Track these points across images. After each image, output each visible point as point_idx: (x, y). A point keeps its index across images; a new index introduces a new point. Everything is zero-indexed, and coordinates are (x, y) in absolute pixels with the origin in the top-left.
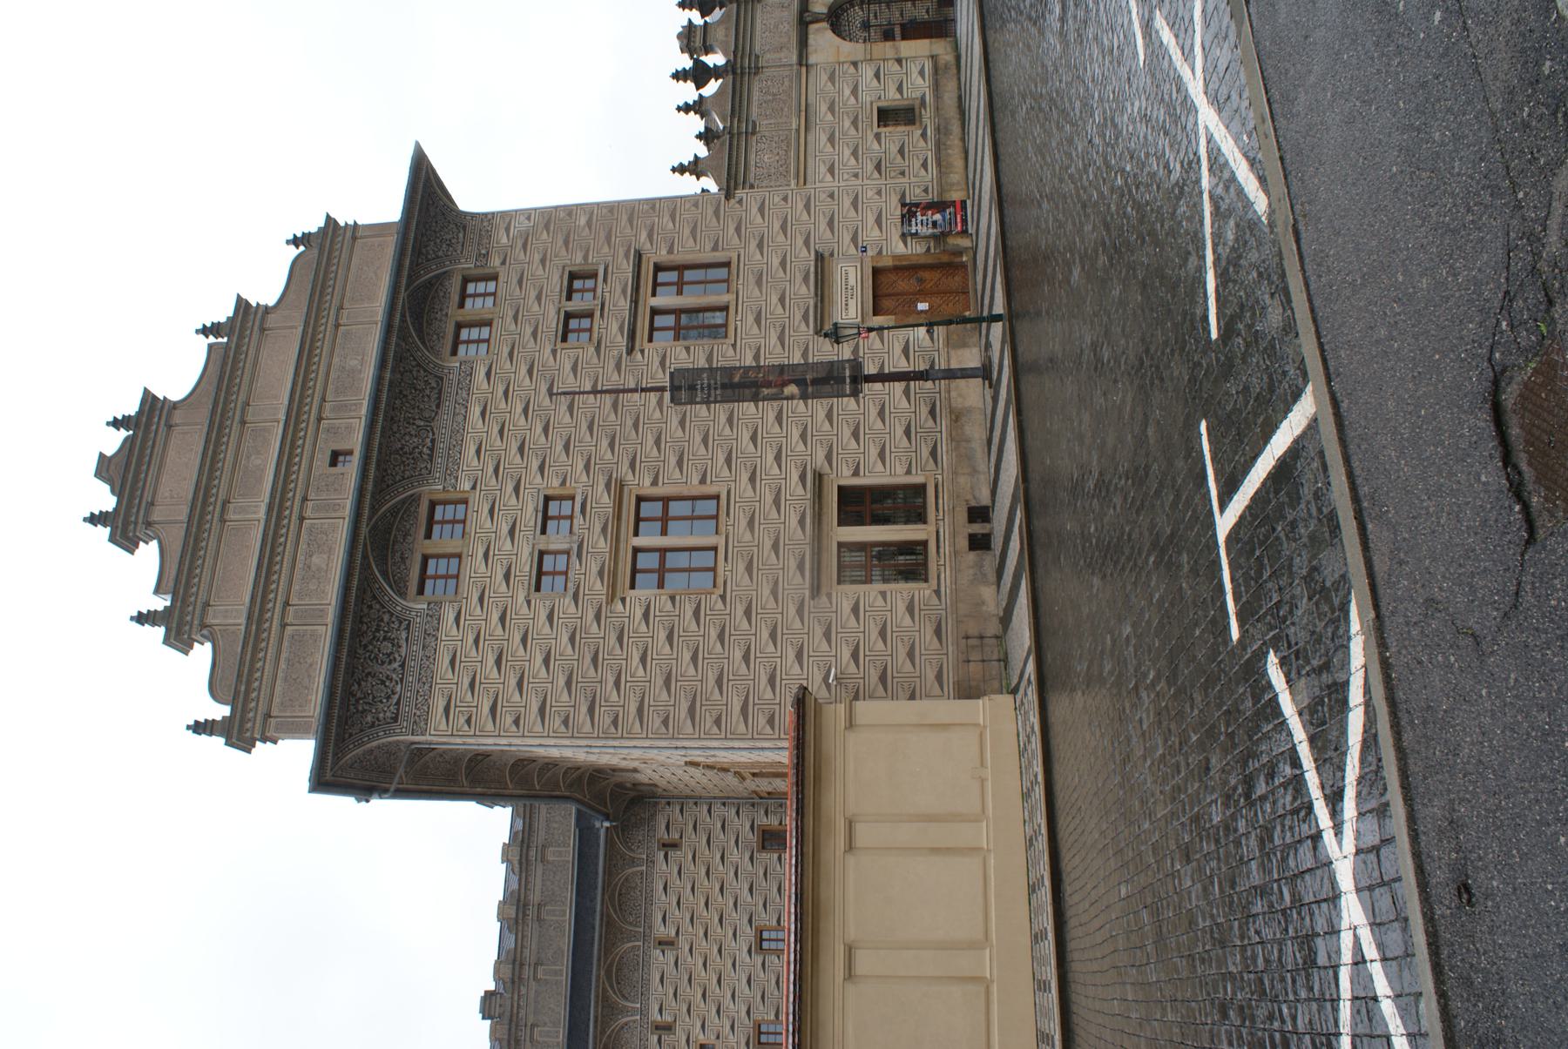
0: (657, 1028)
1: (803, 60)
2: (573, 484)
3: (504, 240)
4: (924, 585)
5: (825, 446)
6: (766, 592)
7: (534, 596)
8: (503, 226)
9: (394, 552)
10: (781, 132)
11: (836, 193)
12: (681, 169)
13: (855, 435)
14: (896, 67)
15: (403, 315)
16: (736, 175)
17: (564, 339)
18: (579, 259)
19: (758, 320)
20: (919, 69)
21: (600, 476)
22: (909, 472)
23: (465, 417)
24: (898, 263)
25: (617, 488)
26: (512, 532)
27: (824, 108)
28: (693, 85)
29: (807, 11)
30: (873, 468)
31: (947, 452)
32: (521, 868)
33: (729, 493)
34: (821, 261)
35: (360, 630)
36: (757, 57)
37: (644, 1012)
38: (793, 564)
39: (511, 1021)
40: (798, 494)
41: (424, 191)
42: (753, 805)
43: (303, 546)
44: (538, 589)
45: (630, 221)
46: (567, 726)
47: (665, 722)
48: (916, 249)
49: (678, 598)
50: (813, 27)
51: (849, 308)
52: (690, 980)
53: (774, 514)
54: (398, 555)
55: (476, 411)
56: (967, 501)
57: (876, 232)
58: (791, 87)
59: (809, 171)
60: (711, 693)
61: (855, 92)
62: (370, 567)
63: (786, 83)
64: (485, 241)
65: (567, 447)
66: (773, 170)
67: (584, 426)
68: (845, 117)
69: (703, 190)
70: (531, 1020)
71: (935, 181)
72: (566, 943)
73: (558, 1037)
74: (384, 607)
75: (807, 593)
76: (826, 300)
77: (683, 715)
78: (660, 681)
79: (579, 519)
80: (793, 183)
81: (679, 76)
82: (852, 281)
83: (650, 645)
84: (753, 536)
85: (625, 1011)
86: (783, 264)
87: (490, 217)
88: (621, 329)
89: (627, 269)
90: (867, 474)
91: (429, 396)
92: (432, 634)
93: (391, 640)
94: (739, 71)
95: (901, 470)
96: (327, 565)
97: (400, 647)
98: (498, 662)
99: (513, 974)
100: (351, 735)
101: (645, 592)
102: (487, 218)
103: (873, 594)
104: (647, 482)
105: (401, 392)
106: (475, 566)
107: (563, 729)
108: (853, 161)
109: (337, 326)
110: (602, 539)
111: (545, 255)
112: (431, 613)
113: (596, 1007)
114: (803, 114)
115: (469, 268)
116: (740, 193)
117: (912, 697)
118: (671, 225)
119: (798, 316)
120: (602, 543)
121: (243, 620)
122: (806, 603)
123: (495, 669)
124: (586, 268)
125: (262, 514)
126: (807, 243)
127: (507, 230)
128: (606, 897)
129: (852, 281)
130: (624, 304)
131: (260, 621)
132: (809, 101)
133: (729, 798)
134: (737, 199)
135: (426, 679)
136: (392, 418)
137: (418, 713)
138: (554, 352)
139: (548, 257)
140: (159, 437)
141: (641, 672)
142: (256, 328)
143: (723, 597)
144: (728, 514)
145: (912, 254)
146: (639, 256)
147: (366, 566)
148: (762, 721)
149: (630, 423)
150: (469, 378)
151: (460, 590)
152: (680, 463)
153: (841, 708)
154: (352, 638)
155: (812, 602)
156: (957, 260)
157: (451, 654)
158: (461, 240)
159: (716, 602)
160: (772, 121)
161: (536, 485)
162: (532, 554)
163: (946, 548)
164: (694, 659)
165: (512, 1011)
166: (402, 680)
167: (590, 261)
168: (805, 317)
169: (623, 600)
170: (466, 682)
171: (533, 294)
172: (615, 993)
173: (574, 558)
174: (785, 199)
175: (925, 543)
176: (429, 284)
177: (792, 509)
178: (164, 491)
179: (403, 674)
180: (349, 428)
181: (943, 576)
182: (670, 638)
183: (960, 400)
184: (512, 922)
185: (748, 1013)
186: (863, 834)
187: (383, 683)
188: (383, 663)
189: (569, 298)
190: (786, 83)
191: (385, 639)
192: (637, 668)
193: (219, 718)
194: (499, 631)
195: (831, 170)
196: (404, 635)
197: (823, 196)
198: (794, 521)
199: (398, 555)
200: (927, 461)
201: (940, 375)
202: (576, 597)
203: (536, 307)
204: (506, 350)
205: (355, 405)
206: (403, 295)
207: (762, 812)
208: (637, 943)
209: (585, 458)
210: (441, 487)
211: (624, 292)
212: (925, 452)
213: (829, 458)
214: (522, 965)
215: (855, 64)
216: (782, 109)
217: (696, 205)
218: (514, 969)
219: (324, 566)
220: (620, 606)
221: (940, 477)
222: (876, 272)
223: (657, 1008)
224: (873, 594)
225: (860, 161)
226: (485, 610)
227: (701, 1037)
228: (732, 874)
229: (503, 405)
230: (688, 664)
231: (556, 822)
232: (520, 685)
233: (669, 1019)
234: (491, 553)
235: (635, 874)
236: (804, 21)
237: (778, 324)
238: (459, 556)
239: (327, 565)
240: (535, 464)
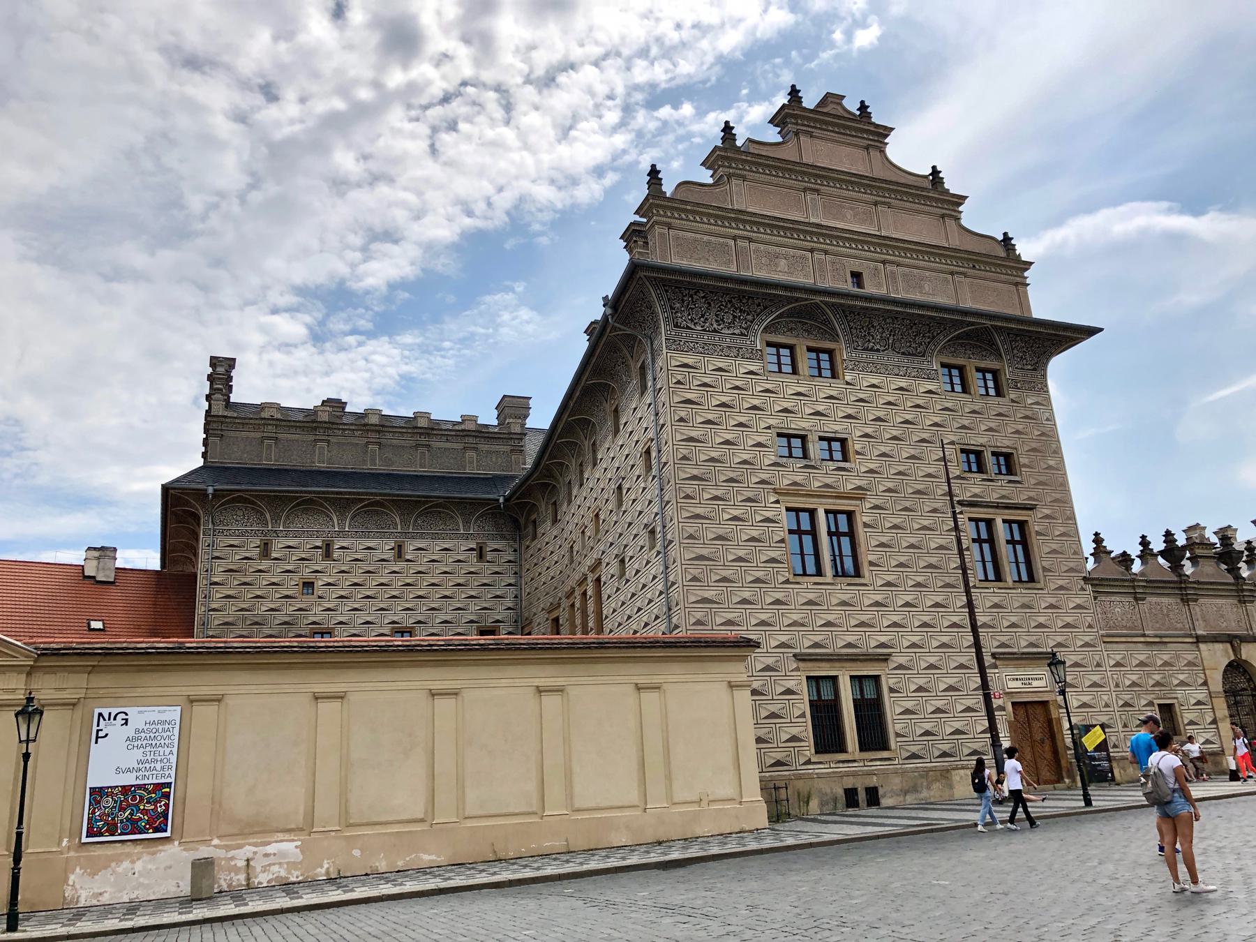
0: (328, 545)
1: (1199, 640)
2: (858, 460)
3: (1030, 401)
4: (813, 751)
5: (909, 663)
6: (795, 617)
7: (773, 432)
8: (1039, 399)
9: (795, 322)
10: (1139, 621)
11: (1101, 669)
12: (1098, 540)
14: (1209, 720)
15: (972, 324)
16: (1102, 585)
17: (963, 451)
19: (996, 606)
20: (1211, 739)
21: (866, 482)
22: (898, 735)
23: (898, 375)
24: (1054, 723)
25: (859, 494)
26: (818, 413)
27: (1166, 657)
28: (1163, 548)
29: (1241, 642)
30: (897, 704)
31: (917, 768)
32: (459, 431)
33: (865, 585)
35: (744, 297)
36: (1196, 600)
37: (342, 534)
38: (817, 639)
39: (333, 423)
40: (871, 642)
41: (1064, 337)
42: (515, 622)
43: (792, 252)
44: (779, 435)
45: (1056, 500)
46: (681, 459)
47: (691, 537)
49: (783, 545)
50: (1228, 645)
52: (369, 572)
53: (854, 622)
54: (793, 325)
55: (903, 385)
56: (882, 786)
58: (1176, 629)
59: (1115, 646)
60: (717, 574)
61: (1182, 683)
62: (789, 303)
63: (1179, 626)
65: (884, 455)
67: (901, 468)
68: (1161, 676)
69: (1087, 558)
70: (333, 440)
71: (1124, 754)
72: (400, 466)
73: (319, 462)
74: (757, 316)
75: (798, 651)
76: (1020, 662)
77: (697, 550)
78: (721, 532)
79: (832, 465)
81: (1168, 535)
82: (1035, 683)
83: (746, 524)
84: (835, 605)
85: (342, 518)
86: (1040, 626)
87: (1045, 389)
88: (975, 495)
89: (1021, 499)
90: (892, 699)
91: (910, 346)
92: (739, 353)
93: (734, 320)
94: (1183, 585)
95: (898, 727)
96: (780, 271)
97: (728, 328)
98: (723, 405)
99: (372, 425)
100: (667, 291)
101: (786, 521)
102: (1041, 387)
103: (801, 706)
104: (865, 519)
105: (915, 324)
106: (792, 386)
107: (680, 456)
108: (1128, 683)
109: (952, 273)
110: (821, 484)
111: (1023, 434)
112: (754, 352)
113: (350, 493)
114: (1157, 640)
115: (1005, 374)
117: (759, 740)
118: (1058, 533)
119: (1004, 639)
120: (817, 484)
122: (790, 650)
123: (719, 403)
124: (1017, 466)
125: (813, 220)
127: (1037, 403)
128: (441, 500)
129: (1035, 683)
130: (994, 497)
131: (735, 220)
132: (1169, 645)
133: (521, 601)
134: (1084, 586)
135: (707, 350)
136: (896, 318)
137: (682, 343)
138: (952, 443)
139: (1022, 436)
140: (859, 140)
141: (726, 516)
142: (944, 211)
143: (787, 582)
144: (849, 585)
145: (1063, 735)
146: (1032, 508)
147: (790, 300)
148: (699, 615)
149: (908, 504)
150: (926, 377)
151: (772, 374)
152: (882, 545)
153: (744, 677)
154: (739, 291)
155: (791, 655)
156: (1064, 774)
157: (726, 368)
158: (1026, 367)
159: (783, 576)
160: (1148, 615)
161: (854, 433)
162: (804, 429)
163: (843, 768)
164: (740, 559)
165: (341, 424)
166: (705, 330)
167: (1023, 469)
168: (1003, 645)
169: (777, 502)
170: (707, 380)
172: (358, 509)
173: (804, 462)
174: (1090, 626)
175: (843, 749)
176: (992, 344)
177: (859, 637)
178: (822, 146)
179: (709, 331)
181: (822, 766)
182: (753, 539)
183: (958, 778)
184: (414, 424)
185: (341, 623)
186: (649, 697)
187: (703, 316)
188: (717, 316)
189: (994, 454)
190: (1179, 626)
191: (734, 317)
192: (729, 513)
193: (664, 188)
194: (746, 405)
195: (1118, 664)
196: (737, 331)
197: (1097, 658)
198: (850, 639)
199: (793, 325)
200: (908, 751)
201: (998, 757)
203: (983, 428)
204: (949, 405)
205: (897, 289)
206: (989, 323)
207: (510, 630)
208: (399, 527)
209: (878, 470)
210: (845, 357)
211: (1003, 497)
212: (914, 749)
213: (900, 667)
214: (379, 432)
215: (1205, 683)
216: (1157, 622)
217: (1075, 553)
218: (376, 425)
219: (779, 269)
220: (772, 499)
221: (896, 762)
222: (1044, 704)
223: (344, 545)
225: (1129, 689)
226: (760, 394)
227: (321, 583)
228: (459, 605)
229: (910, 404)
230: (735, 554)
231: (497, 459)
232: (709, 422)
233: (335, 555)
234: (801, 398)
235: (457, 524)
236: (1233, 640)
237: (995, 622)
238: (795, 371)
239: (780, 271)
240: (869, 431)
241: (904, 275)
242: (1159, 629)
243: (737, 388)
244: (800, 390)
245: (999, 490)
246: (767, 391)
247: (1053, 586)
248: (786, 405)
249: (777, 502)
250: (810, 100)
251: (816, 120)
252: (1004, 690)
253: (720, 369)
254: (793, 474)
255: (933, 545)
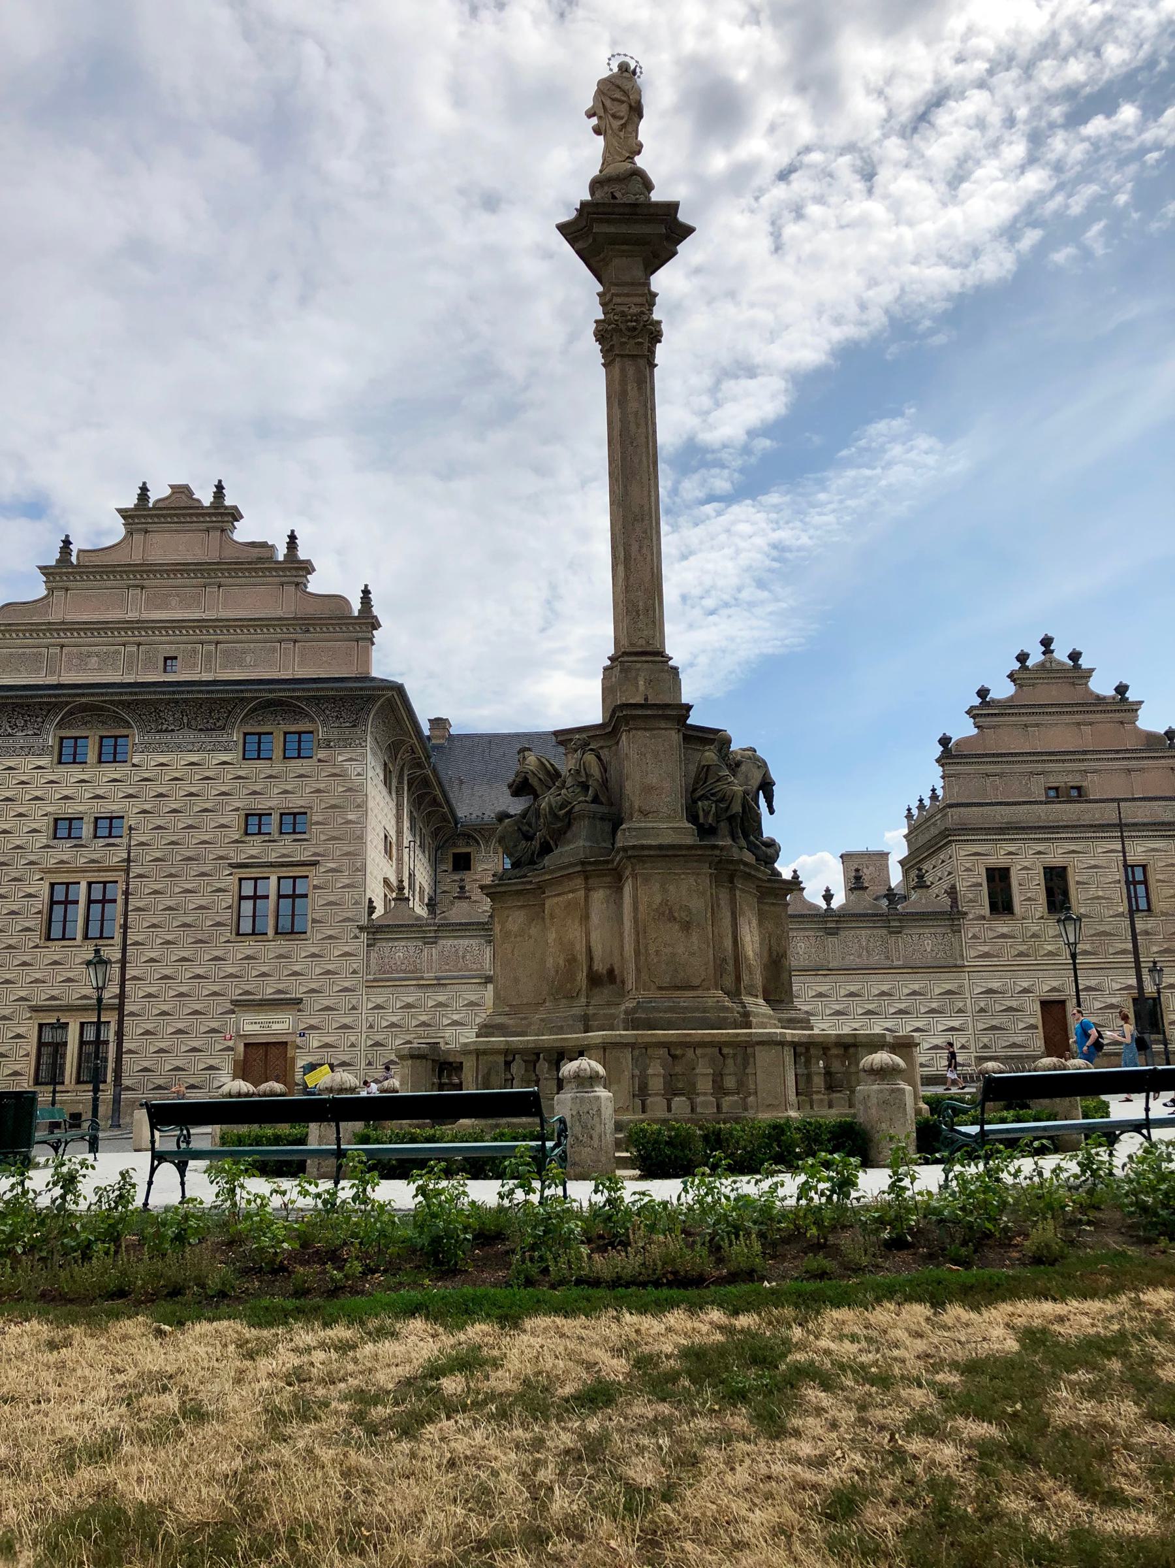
3: (340, 758)
4: (31, 1083)
6: (38, 976)
8: (354, 756)
13: (147, 1033)
18: (315, 819)
19: (248, 958)
27: (441, 999)
34: (295, 1003)
38: (55, 993)
48: (298, 1077)
51: (253, 1025)
55: (194, 758)
57: (316, 1044)
59: (379, 989)
61: (455, 1023)
63: (475, 967)
64: (342, 743)
66: (386, 960)
67: (174, 839)
79: (102, 842)
80: (371, 977)
82: (275, 1026)
88: (252, 857)
89: (305, 856)
92: (30, 751)
106: (76, 773)
108: (385, 1024)
116: (364, 936)
119: (247, 988)
120: (83, 860)
121: (51, 619)
125: (132, 615)
126: (313, 991)
129: (275, 1026)
130: (273, 857)
138: (237, 809)
146: (314, 864)
147: (67, 703)
149: (173, 871)
161: (131, 810)
162: (81, 813)
169: (42, 879)
171: (289, 788)
173: (75, 842)
174: (354, 972)
180: (195, 665)
190: (475, 967)
194: (28, 797)
197: (354, 1002)
202: (48, 846)
206: (271, 696)
211: (284, 856)
220: (38, 877)
224: (28, 1048)
240: (147, 807)
241: (226, 652)
242: (450, 971)
243: (23, 783)
244: (82, 777)
245: (285, 848)
246: (52, 782)
247: (320, 936)
248: (66, 793)
249: (42, 879)
250: (154, 496)
251: (157, 516)
252: (238, 1031)
253: (10, 768)
254: (64, 851)
255: (192, 906)
